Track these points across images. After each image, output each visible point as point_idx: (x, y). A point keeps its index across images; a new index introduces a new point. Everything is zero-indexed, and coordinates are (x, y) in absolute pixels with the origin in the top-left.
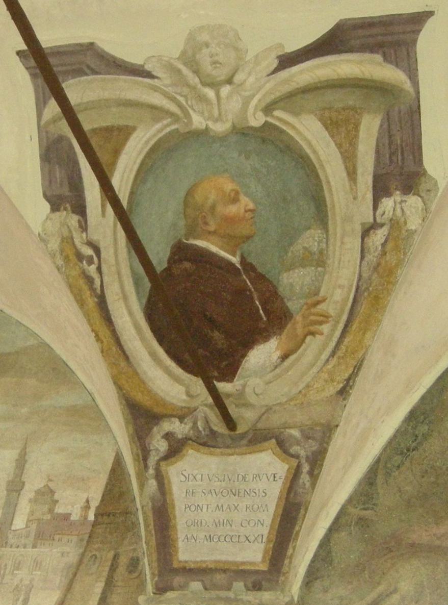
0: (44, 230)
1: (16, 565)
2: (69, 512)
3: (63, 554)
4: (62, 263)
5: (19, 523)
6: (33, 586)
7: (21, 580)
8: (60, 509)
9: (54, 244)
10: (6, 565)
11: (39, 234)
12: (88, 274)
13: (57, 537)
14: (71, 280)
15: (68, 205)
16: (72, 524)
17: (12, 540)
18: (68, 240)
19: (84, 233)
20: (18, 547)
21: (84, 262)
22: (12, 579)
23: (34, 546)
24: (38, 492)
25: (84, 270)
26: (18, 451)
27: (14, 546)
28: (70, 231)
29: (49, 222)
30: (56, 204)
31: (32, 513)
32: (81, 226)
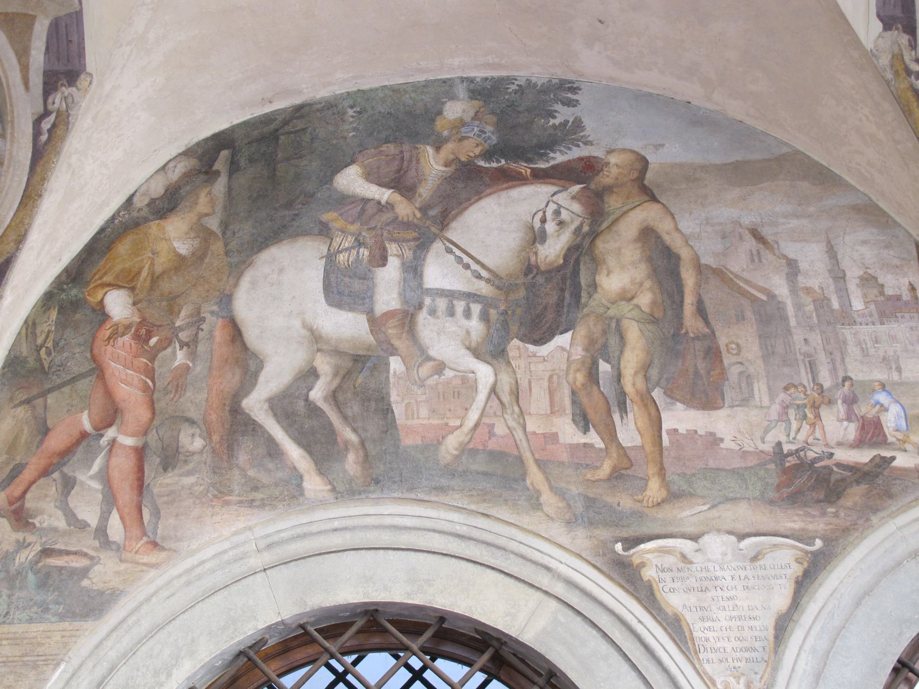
0: (876, 46)
1: (874, 340)
2: (898, 293)
3: (911, 328)
4: (892, 77)
5: (858, 304)
6: (898, 357)
7: (886, 352)
8: (889, 292)
9: (884, 60)
10: (864, 340)
11: (871, 50)
12: (916, 87)
13: (898, 315)
14: (900, 93)
15: (899, 26)
16: (906, 303)
17: (859, 320)
18: (898, 57)
19: (914, 51)
20: (867, 324)
21: (913, 77)
22: (876, 352)
23: (882, 323)
24: (861, 278)
25: (912, 84)
26: (825, 243)
27: (863, 323)
28: (901, 50)
29: (880, 39)
30: (888, 23)
31: (865, 296)
32: (910, 45)
